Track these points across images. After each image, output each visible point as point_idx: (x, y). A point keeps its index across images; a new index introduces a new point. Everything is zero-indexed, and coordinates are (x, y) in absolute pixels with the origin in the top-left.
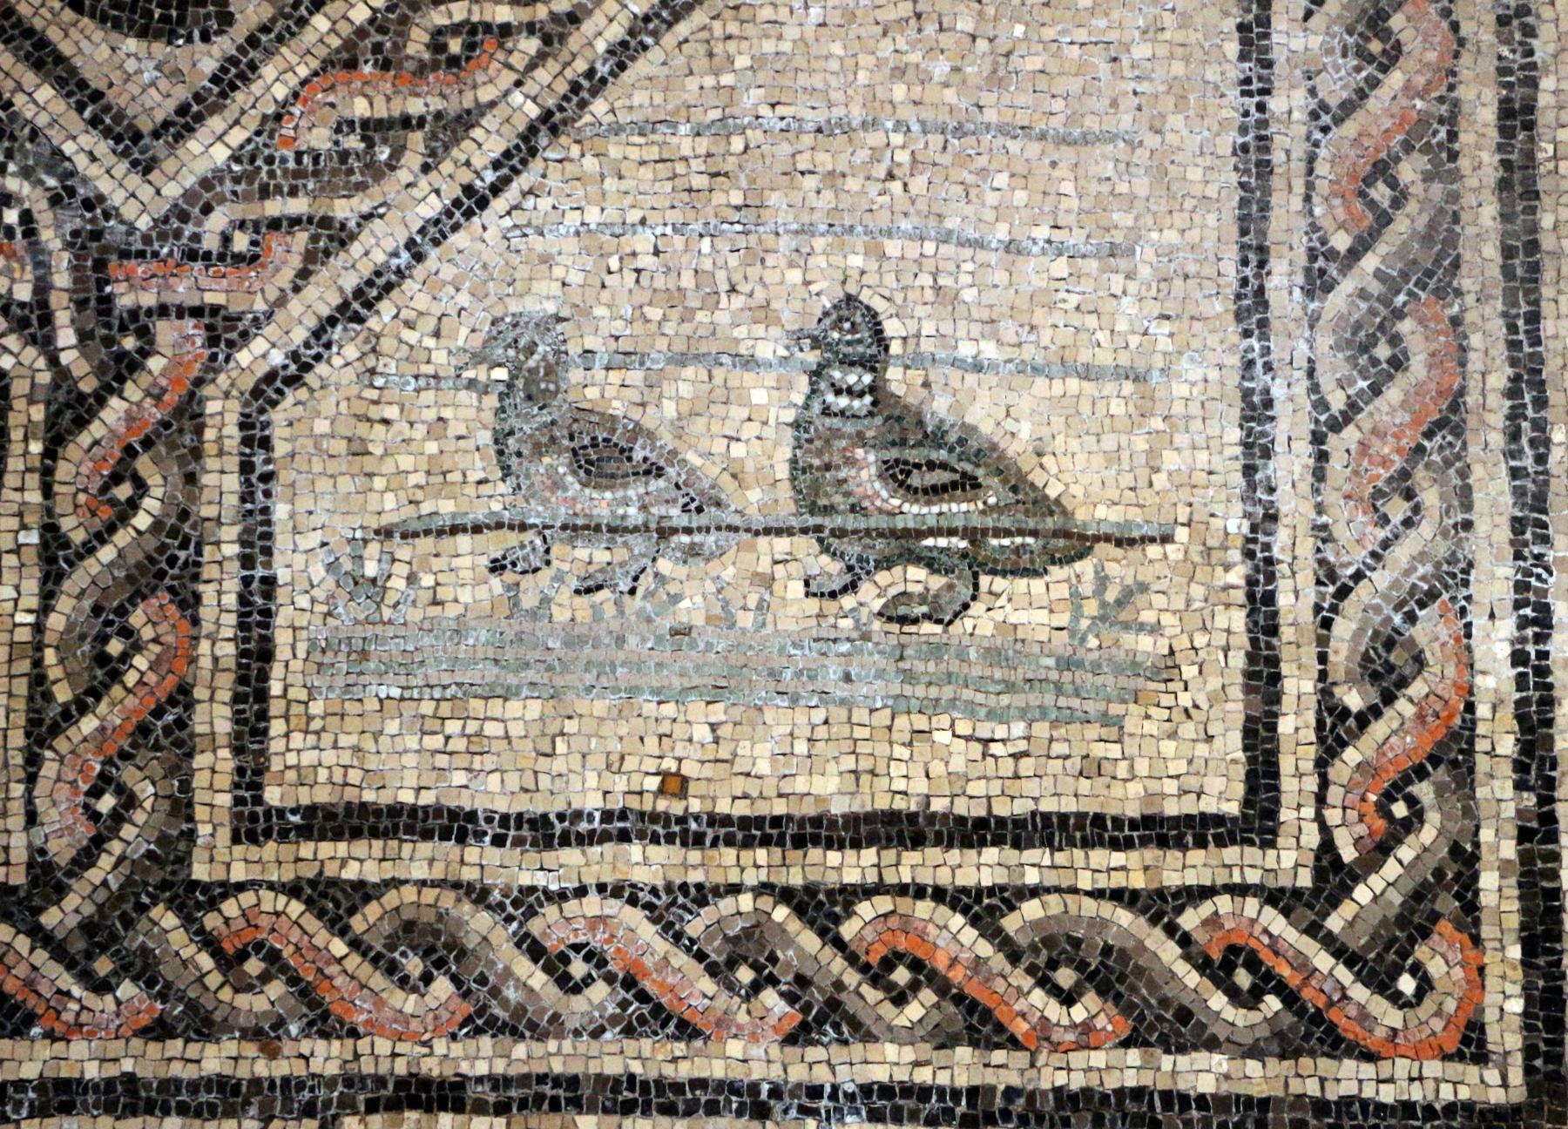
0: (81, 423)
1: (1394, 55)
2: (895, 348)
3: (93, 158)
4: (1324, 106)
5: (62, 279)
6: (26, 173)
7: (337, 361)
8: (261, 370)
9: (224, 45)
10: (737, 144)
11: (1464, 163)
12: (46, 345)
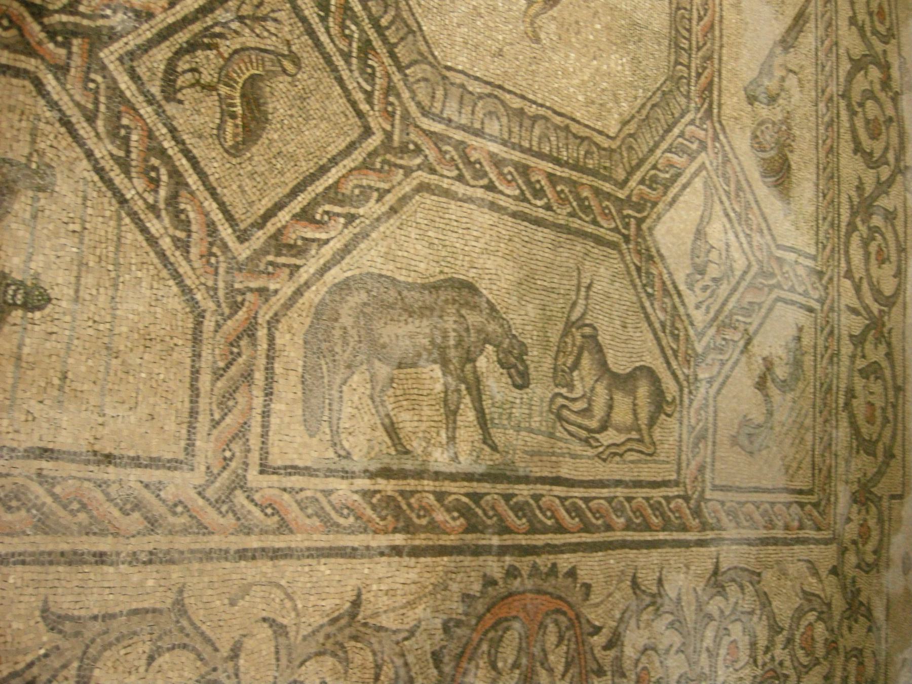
0: (33, 14)
2: (30, 315)
3: (126, 44)
4: (108, 486)
5: (85, 22)
6: (123, 21)
7: (45, 109)
8: (45, 81)
9: (159, 96)
10: (111, 267)
11: (84, 538)
12: (63, 10)
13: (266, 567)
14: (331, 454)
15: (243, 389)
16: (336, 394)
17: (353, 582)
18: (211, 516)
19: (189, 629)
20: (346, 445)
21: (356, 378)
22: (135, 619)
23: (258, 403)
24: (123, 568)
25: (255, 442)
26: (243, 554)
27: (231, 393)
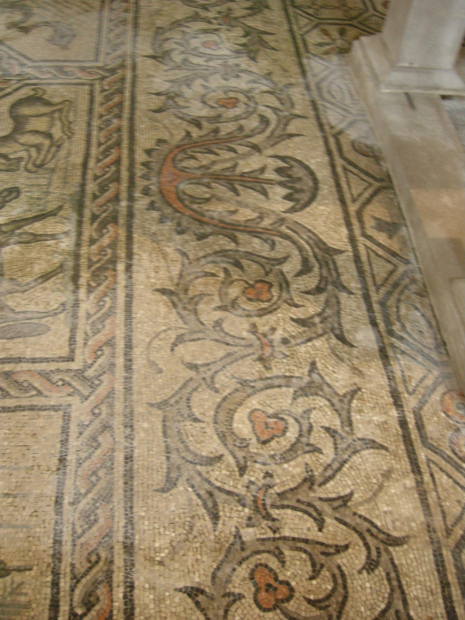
1: (99, 445)
4: (81, 459)
11: (115, 470)
13: (137, 352)
14: (62, 316)
15: (16, 377)
16: (20, 316)
17: (149, 295)
18: (102, 390)
19: (177, 398)
20: (56, 306)
21: (9, 304)
22: (169, 432)
23: (25, 366)
24: (135, 443)
25: (53, 366)
26: (128, 368)
27: (18, 385)
